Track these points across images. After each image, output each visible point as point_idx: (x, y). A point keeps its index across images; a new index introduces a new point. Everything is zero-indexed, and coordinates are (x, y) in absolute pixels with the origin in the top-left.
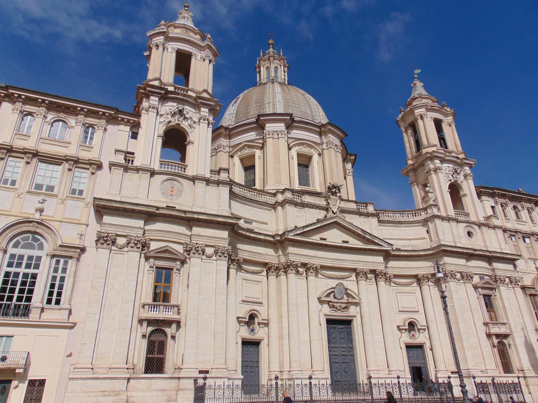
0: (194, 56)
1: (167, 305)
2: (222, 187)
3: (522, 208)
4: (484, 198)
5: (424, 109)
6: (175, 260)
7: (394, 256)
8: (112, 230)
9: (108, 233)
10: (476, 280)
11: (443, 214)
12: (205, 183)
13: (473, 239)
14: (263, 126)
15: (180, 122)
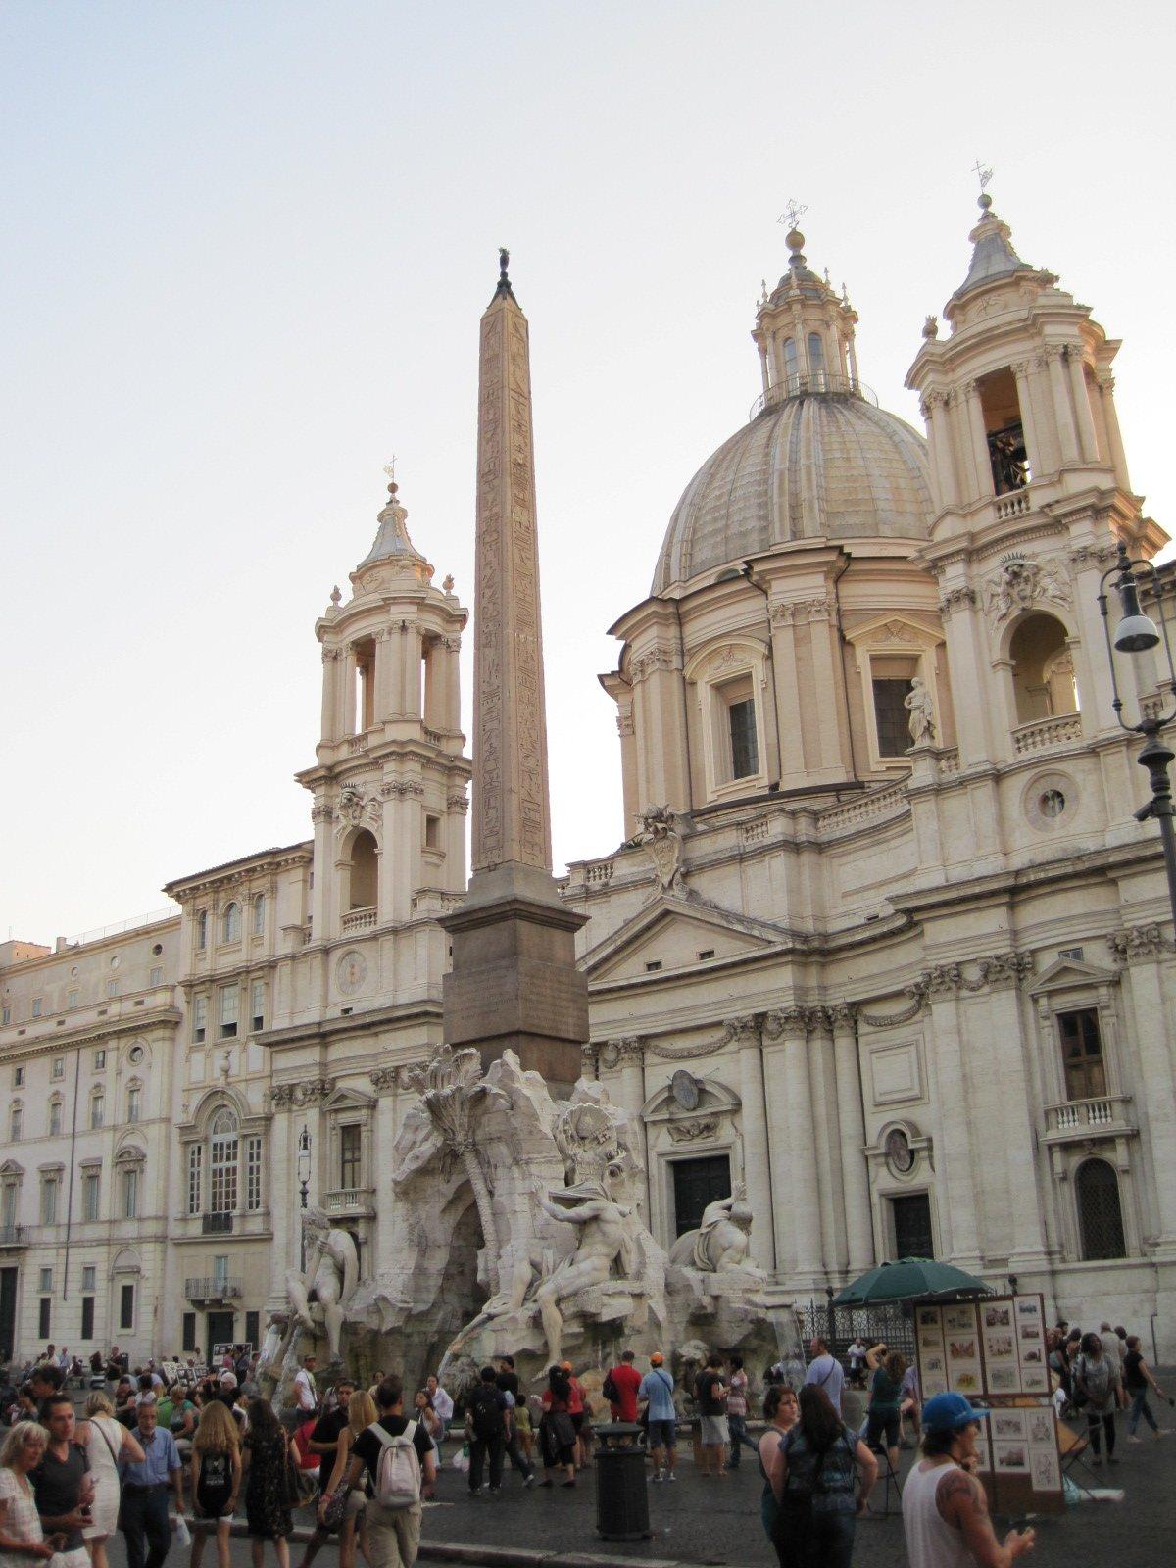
5: (930, 378)
8: (284, 1080)
9: (280, 1087)
10: (1048, 961)
12: (391, 937)
15: (356, 822)
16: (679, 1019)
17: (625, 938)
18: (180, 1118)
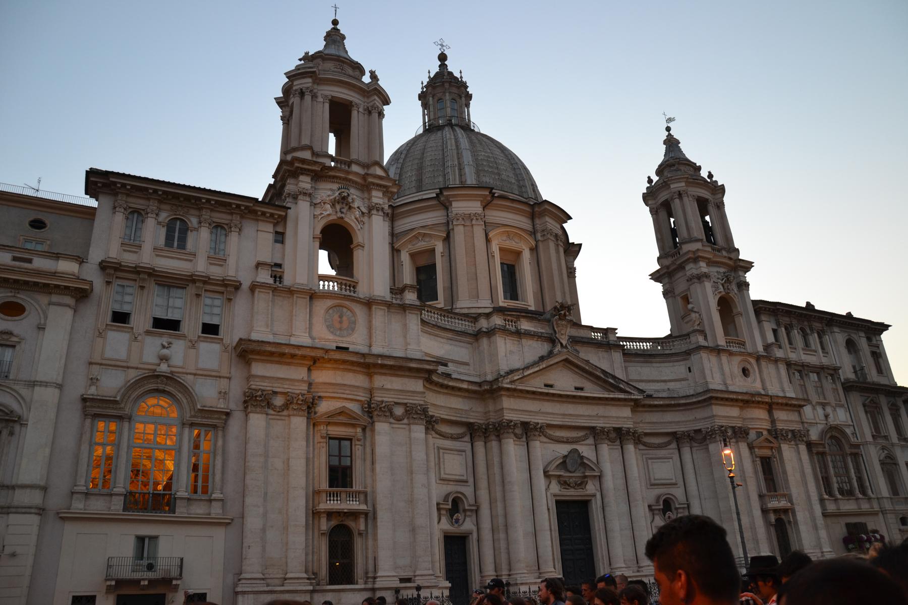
0: (355, 108)
1: (350, 492)
2: (410, 315)
3: (810, 330)
4: (763, 318)
5: (683, 184)
6: (354, 426)
7: (644, 406)
8: (266, 385)
10: (752, 435)
11: (711, 344)
12: (386, 308)
13: (749, 379)
14: (447, 204)
15: (343, 215)
16: (567, 420)
17: (544, 366)
18: (78, 387)
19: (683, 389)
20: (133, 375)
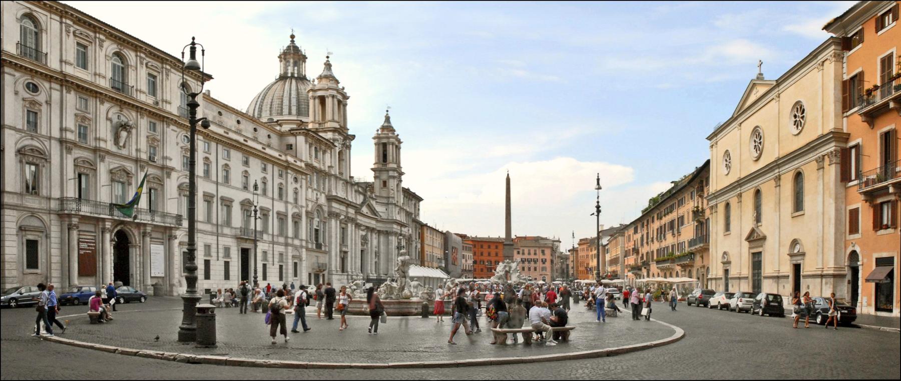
6: (346, 224)
19: (384, 216)
20: (313, 203)
